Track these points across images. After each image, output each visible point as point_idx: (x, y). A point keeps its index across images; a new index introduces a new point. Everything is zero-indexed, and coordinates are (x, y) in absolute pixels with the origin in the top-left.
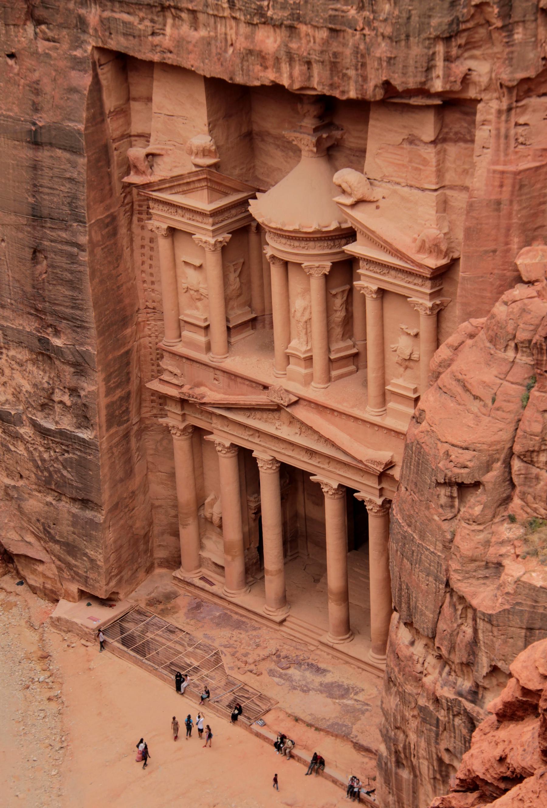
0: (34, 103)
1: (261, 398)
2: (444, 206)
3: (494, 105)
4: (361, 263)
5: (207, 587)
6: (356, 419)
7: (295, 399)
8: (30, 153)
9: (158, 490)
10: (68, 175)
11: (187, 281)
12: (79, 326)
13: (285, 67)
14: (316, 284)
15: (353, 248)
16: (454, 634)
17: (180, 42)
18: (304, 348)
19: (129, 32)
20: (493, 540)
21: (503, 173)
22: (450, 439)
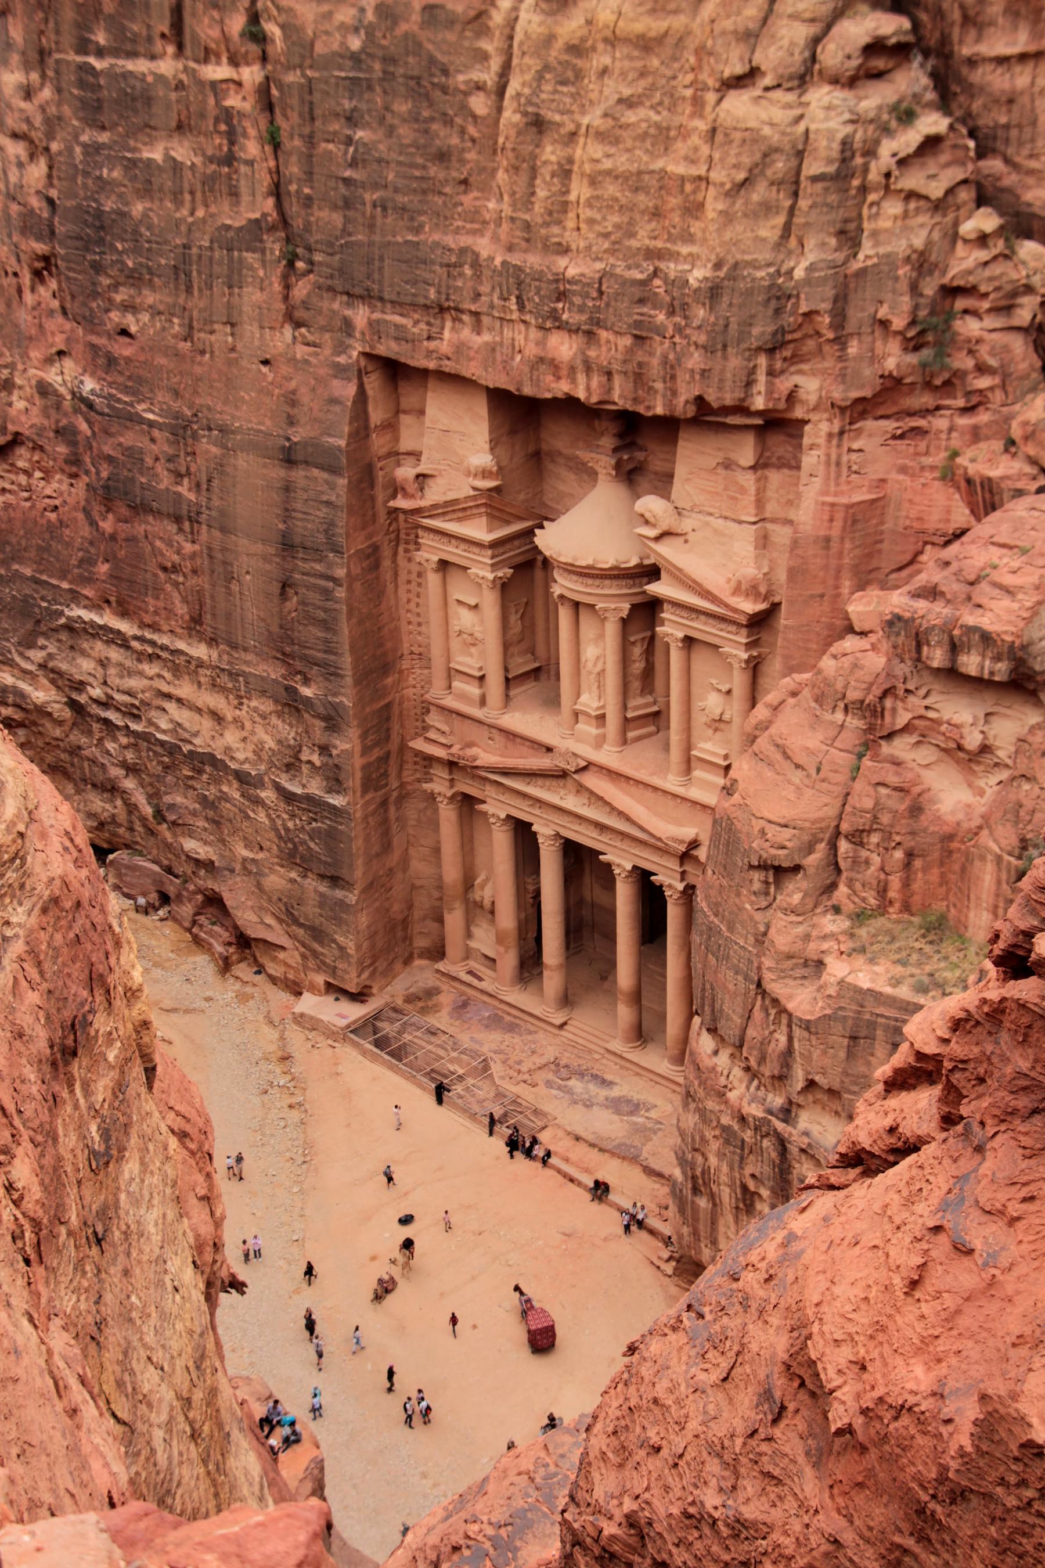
0: (289, 416)
1: (543, 762)
2: (764, 542)
3: (824, 427)
4: (665, 606)
5: (475, 982)
6: (656, 789)
7: (584, 764)
8: (282, 473)
9: (419, 867)
10: (325, 498)
11: (460, 623)
12: (332, 673)
13: (581, 378)
14: (612, 630)
15: (656, 588)
16: (765, 1043)
17: (460, 348)
18: (596, 704)
19: (401, 336)
20: (814, 933)
21: (833, 505)
22: (767, 814)
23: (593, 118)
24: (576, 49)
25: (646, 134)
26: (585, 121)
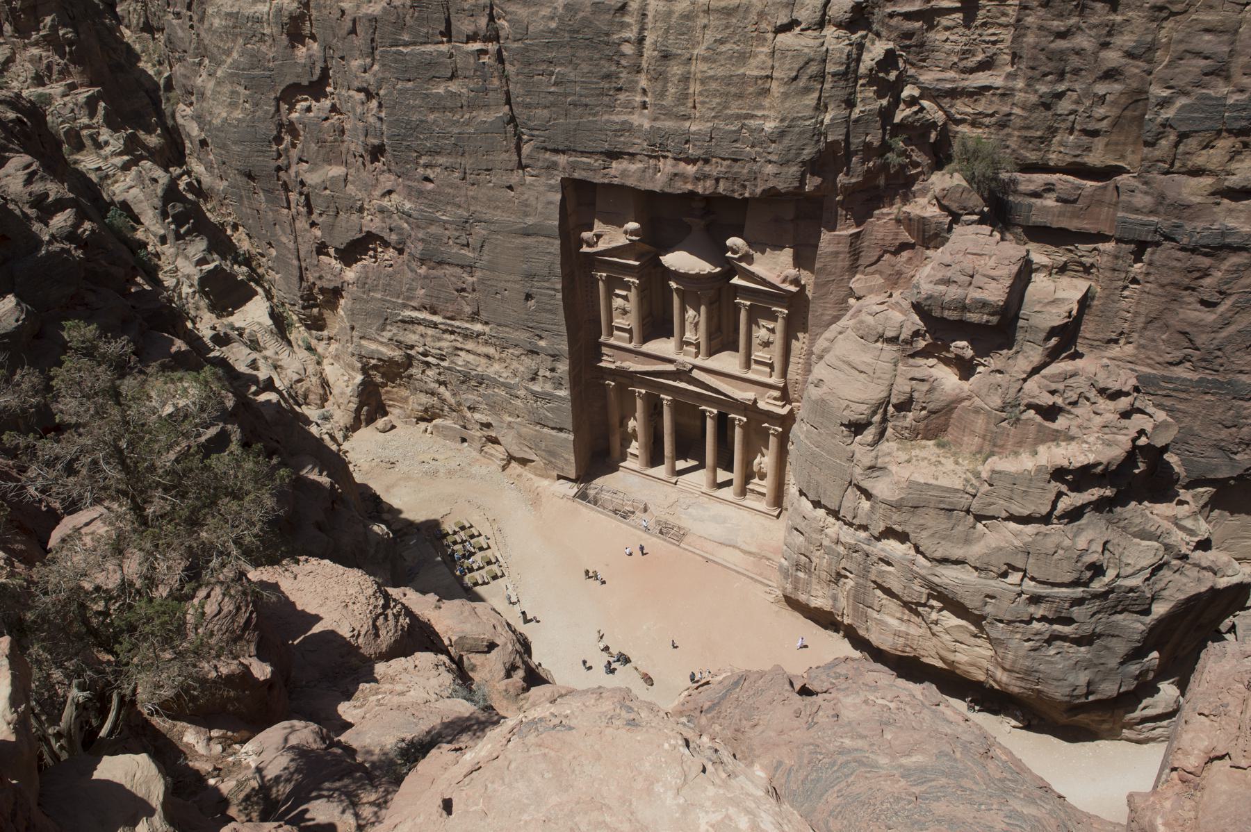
19: (588, 168)
23: (700, 50)
24: (687, 17)
25: (731, 58)
26: (696, 52)
